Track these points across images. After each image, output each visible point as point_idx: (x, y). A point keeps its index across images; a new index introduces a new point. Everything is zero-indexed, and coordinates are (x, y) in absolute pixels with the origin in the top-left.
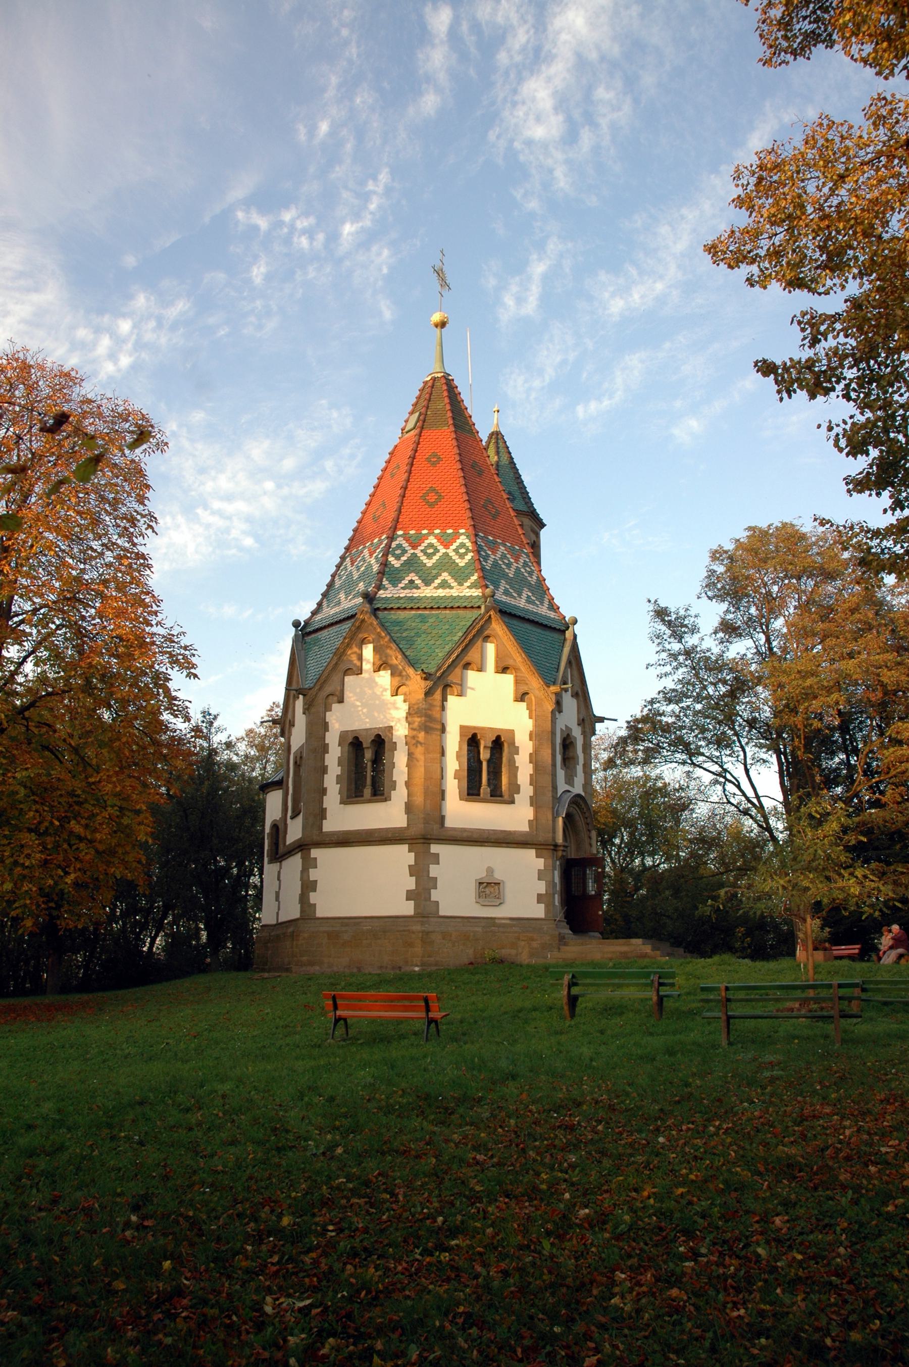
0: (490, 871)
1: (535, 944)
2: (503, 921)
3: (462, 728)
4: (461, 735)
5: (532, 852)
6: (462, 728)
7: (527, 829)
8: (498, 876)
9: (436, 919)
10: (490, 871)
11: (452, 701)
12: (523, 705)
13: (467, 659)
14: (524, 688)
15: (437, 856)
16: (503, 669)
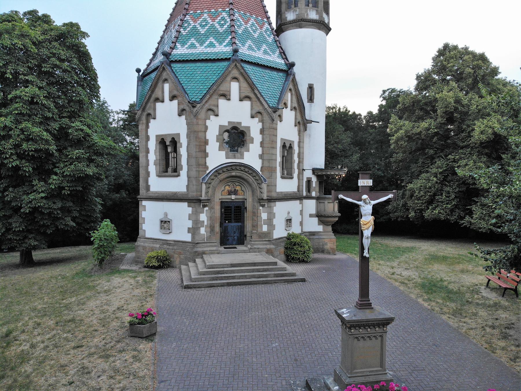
0: (166, 214)
1: (182, 257)
2: (171, 242)
3: (157, 136)
4: (156, 141)
5: (186, 204)
6: (157, 136)
7: (186, 191)
8: (170, 217)
9: (144, 239)
10: (166, 214)
11: (152, 123)
12: (183, 117)
13: (154, 96)
14: (182, 107)
15: (145, 206)
16: (173, 98)
